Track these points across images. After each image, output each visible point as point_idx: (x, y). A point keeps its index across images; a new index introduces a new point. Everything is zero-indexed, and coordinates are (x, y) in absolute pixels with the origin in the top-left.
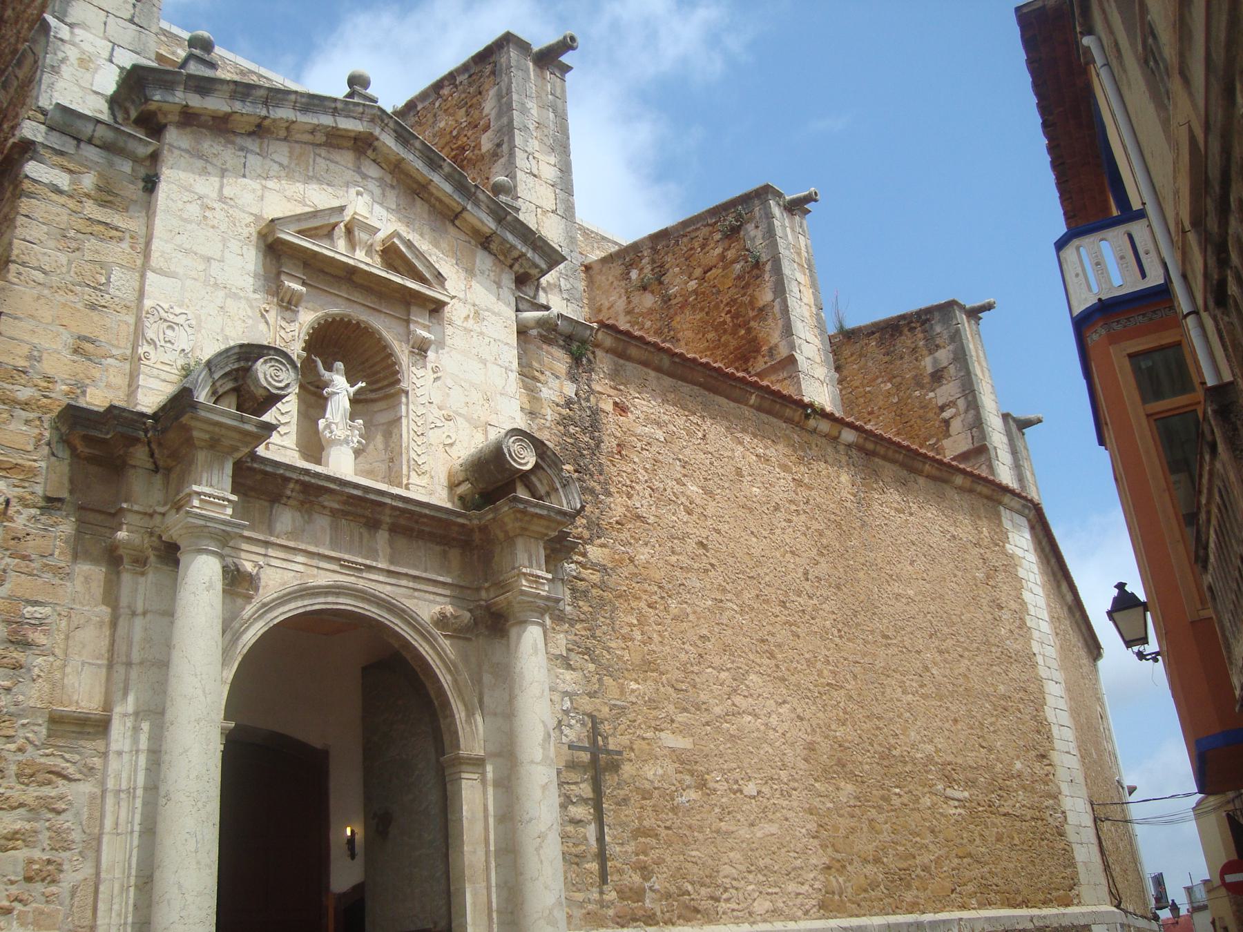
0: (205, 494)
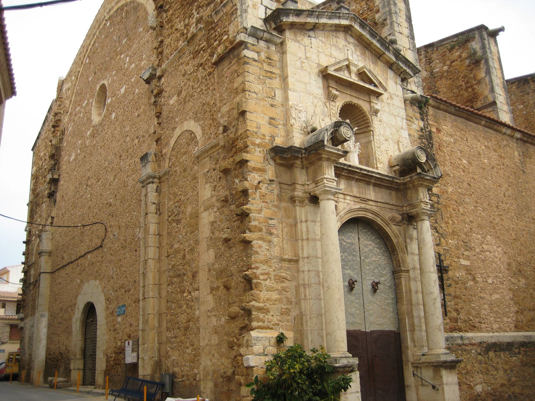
0: (328, 178)
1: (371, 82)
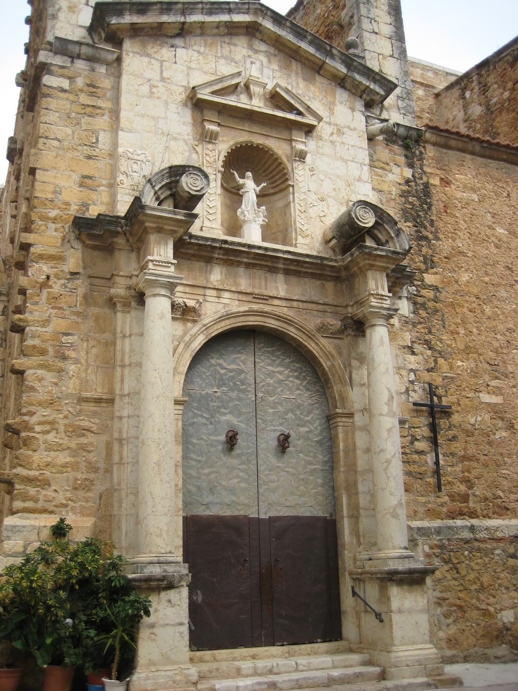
0: (156, 261)
1: (291, 108)
